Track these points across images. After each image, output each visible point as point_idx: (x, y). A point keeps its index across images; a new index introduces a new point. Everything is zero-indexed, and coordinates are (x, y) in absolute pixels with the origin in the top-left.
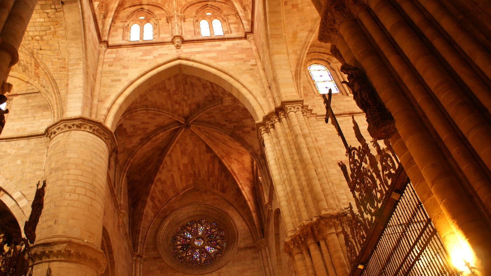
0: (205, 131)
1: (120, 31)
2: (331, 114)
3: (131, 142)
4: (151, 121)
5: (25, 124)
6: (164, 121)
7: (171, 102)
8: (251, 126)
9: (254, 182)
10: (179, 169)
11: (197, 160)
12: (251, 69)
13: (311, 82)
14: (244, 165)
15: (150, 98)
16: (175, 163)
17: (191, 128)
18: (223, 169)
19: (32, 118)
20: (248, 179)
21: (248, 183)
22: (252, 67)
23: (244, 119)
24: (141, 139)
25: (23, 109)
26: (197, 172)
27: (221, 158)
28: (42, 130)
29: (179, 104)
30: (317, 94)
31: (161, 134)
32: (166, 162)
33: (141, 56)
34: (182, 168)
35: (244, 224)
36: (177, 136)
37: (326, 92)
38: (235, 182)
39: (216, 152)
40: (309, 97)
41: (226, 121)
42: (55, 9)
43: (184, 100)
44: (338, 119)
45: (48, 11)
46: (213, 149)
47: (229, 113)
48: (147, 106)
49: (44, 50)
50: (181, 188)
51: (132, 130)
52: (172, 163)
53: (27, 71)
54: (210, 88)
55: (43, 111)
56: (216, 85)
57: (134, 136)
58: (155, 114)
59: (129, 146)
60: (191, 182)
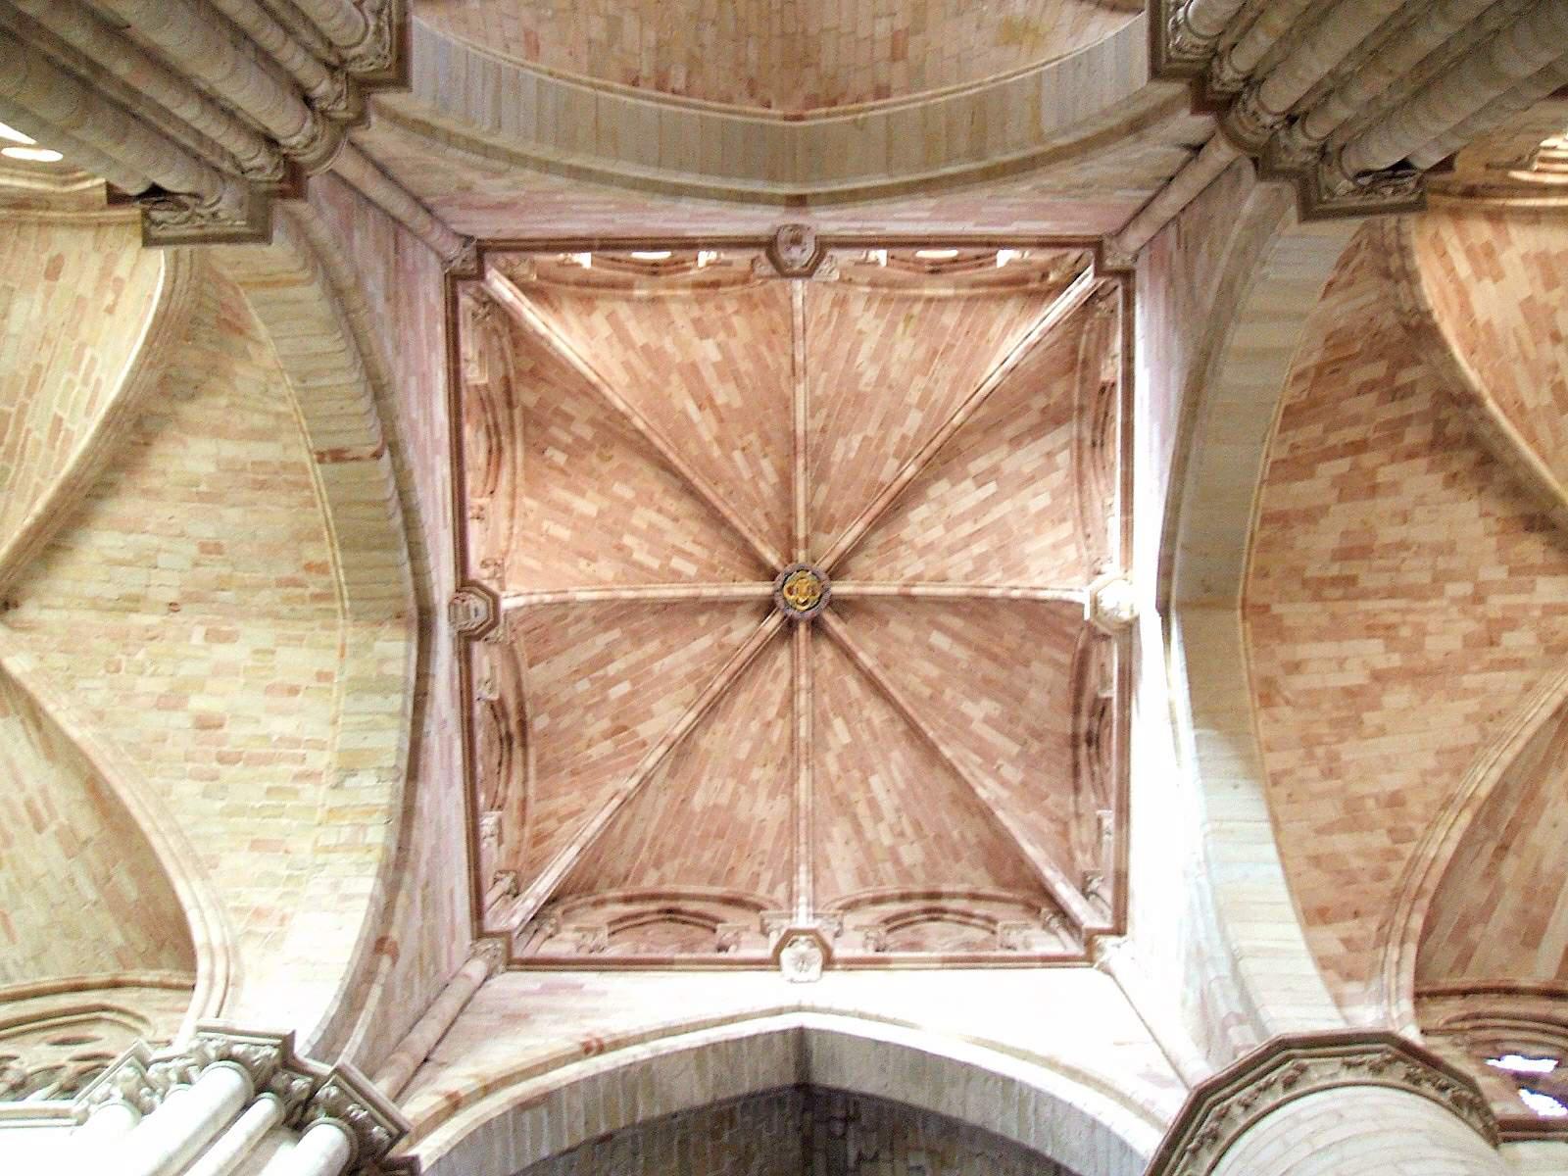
7: (1475, 667)
42: (846, 1120)
43: (1478, 598)
45: (852, 1154)
54: (1368, 460)
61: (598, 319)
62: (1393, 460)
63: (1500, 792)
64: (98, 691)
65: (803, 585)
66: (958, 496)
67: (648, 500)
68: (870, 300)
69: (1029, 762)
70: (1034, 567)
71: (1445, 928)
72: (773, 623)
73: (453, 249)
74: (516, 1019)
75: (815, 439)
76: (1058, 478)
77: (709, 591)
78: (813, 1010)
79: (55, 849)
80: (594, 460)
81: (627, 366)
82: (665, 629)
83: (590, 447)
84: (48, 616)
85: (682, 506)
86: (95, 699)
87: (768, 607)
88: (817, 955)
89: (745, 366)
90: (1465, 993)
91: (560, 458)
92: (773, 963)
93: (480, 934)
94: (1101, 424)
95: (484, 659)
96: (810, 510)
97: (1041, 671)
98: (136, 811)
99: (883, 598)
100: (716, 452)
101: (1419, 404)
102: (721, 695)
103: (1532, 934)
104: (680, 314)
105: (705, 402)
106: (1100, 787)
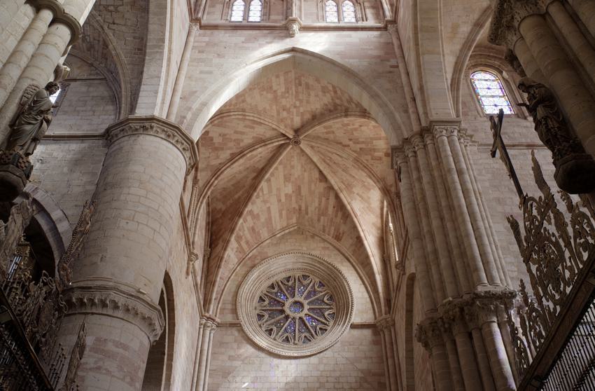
0: (319, 151)
1: (219, 7)
2: (500, 145)
4: (247, 130)
5: (81, 119)
6: (265, 132)
8: (385, 151)
10: (279, 201)
11: (304, 191)
12: (390, 72)
13: (474, 96)
14: (369, 204)
15: (249, 100)
16: (274, 191)
17: (301, 145)
18: (341, 206)
19: (91, 113)
20: (373, 224)
22: (392, 69)
23: (376, 139)
24: (232, 154)
25: (81, 99)
26: (303, 208)
27: (339, 191)
28: (101, 130)
29: (289, 111)
30: (481, 114)
31: (260, 150)
32: (262, 189)
33: (243, 42)
34: (283, 200)
36: (281, 154)
37: (496, 112)
38: (355, 227)
39: (333, 182)
40: (469, 117)
41: (350, 140)
43: (295, 107)
44: (510, 152)
46: (329, 177)
47: (356, 129)
48: (244, 110)
49: (117, 24)
50: (279, 228)
51: (221, 141)
52: (270, 191)
53: (92, 50)
54: (332, 93)
55: (106, 105)
56: (340, 89)
57: (222, 149)
58: (254, 122)
59: (215, 162)
60: (294, 220)
62: (332, 97)
101: (346, 104)
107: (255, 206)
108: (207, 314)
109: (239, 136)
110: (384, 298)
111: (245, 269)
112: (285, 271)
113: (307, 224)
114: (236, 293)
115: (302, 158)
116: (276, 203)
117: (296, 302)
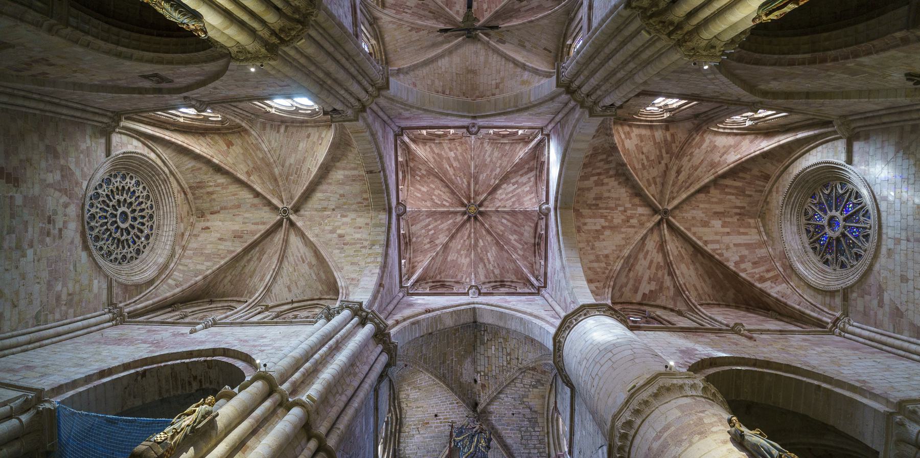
3: (668, 288)
4: (649, 257)
9: (758, 134)
16: (718, 238)
21: (757, 142)
26: (738, 211)
32: (714, 250)
34: (727, 230)
35: (814, 152)
36: (678, 228)
50: (758, 237)
51: (655, 283)
52: (718, 242)
57: (662, 282)
59: (672, 292)
60: (752, 221)
61: (427, 147)
63: (629, 256)
64: (317, 230)
65: (473, 208)
66: (509, 188)
67: (438, 188)
68: (489, 143)
69: (525, 250)
70: (526, 204)
71: (617, 288)
72: (466, 217)
73: (396, 129)
74: (410, 305)
75: (476, 174)
76: (531, 184)
77: (452, 209)
78: (477, 303)
79: (307, 267)
80: (426, 179)
81: (434, 158)
82: (442, 218)
83: (425, 176)
84: (306, 213)
85: (446, 190)
86: (316, 232)
87: (464, 213)
88: (477, 291)
89: (460, 158)
90: (621, 303)
91: (418, 178)
92: (467, 294)
93: (401, 287)
94: (541, 172)
95: (402, 223)
96: (474, 191)
97: (527, 228)
98: (325, 257)
99: (491, 211)
100: (453, 177)
102: (454, 233)
103: (636, 290)
104: (446, 145)
105: (451, 166)
106: (540, 255)
107: (731, 260)
108: (829, 326)
109: (654, 266)
110: (821, 128)
111: (794, 276)
112: (799, 234)
113: (755, 209)
114: (816, 289)
115: (685, 208)
116: (731, 237)
117: (830, 225)
